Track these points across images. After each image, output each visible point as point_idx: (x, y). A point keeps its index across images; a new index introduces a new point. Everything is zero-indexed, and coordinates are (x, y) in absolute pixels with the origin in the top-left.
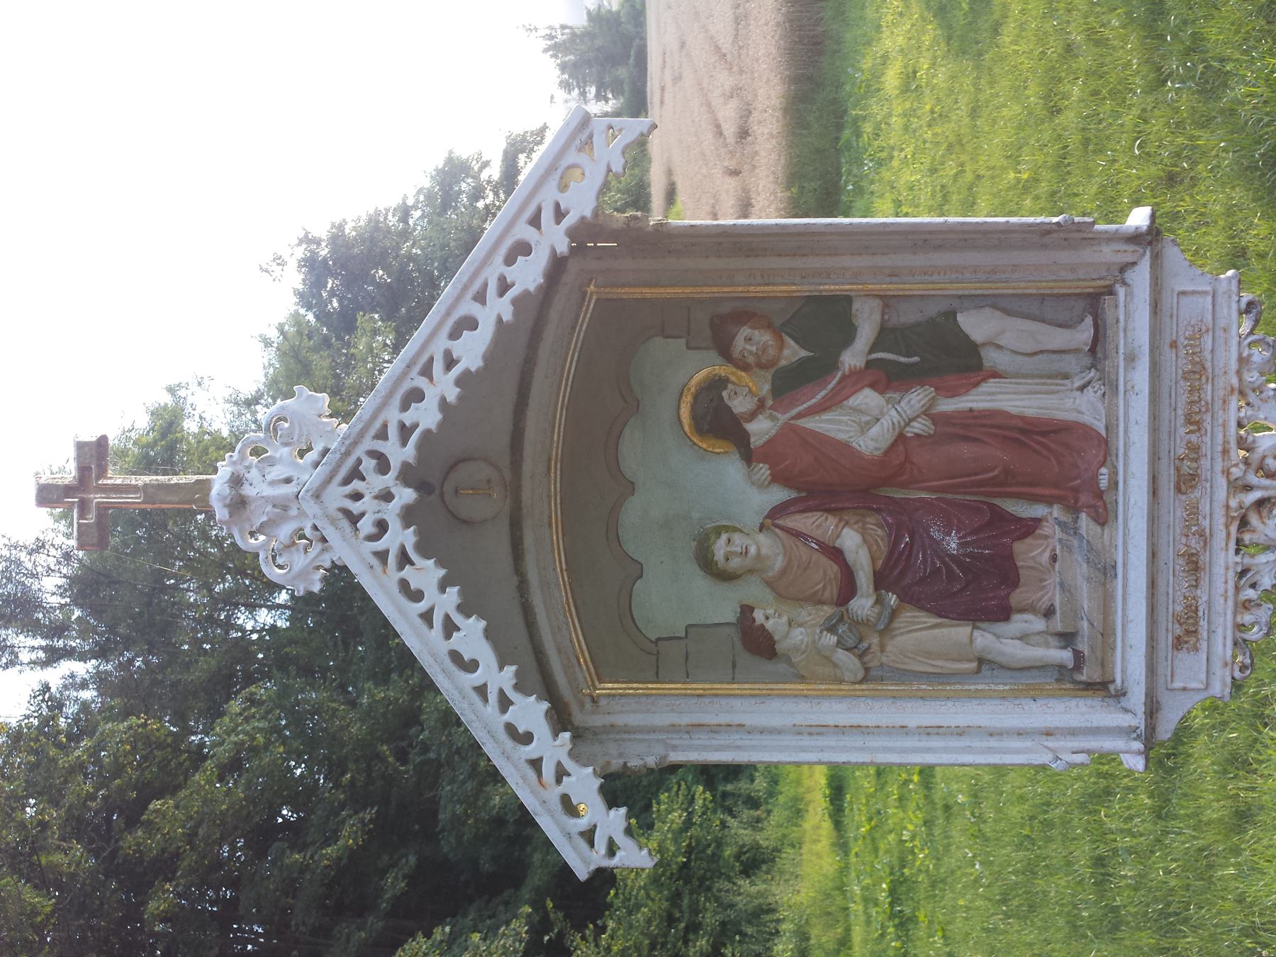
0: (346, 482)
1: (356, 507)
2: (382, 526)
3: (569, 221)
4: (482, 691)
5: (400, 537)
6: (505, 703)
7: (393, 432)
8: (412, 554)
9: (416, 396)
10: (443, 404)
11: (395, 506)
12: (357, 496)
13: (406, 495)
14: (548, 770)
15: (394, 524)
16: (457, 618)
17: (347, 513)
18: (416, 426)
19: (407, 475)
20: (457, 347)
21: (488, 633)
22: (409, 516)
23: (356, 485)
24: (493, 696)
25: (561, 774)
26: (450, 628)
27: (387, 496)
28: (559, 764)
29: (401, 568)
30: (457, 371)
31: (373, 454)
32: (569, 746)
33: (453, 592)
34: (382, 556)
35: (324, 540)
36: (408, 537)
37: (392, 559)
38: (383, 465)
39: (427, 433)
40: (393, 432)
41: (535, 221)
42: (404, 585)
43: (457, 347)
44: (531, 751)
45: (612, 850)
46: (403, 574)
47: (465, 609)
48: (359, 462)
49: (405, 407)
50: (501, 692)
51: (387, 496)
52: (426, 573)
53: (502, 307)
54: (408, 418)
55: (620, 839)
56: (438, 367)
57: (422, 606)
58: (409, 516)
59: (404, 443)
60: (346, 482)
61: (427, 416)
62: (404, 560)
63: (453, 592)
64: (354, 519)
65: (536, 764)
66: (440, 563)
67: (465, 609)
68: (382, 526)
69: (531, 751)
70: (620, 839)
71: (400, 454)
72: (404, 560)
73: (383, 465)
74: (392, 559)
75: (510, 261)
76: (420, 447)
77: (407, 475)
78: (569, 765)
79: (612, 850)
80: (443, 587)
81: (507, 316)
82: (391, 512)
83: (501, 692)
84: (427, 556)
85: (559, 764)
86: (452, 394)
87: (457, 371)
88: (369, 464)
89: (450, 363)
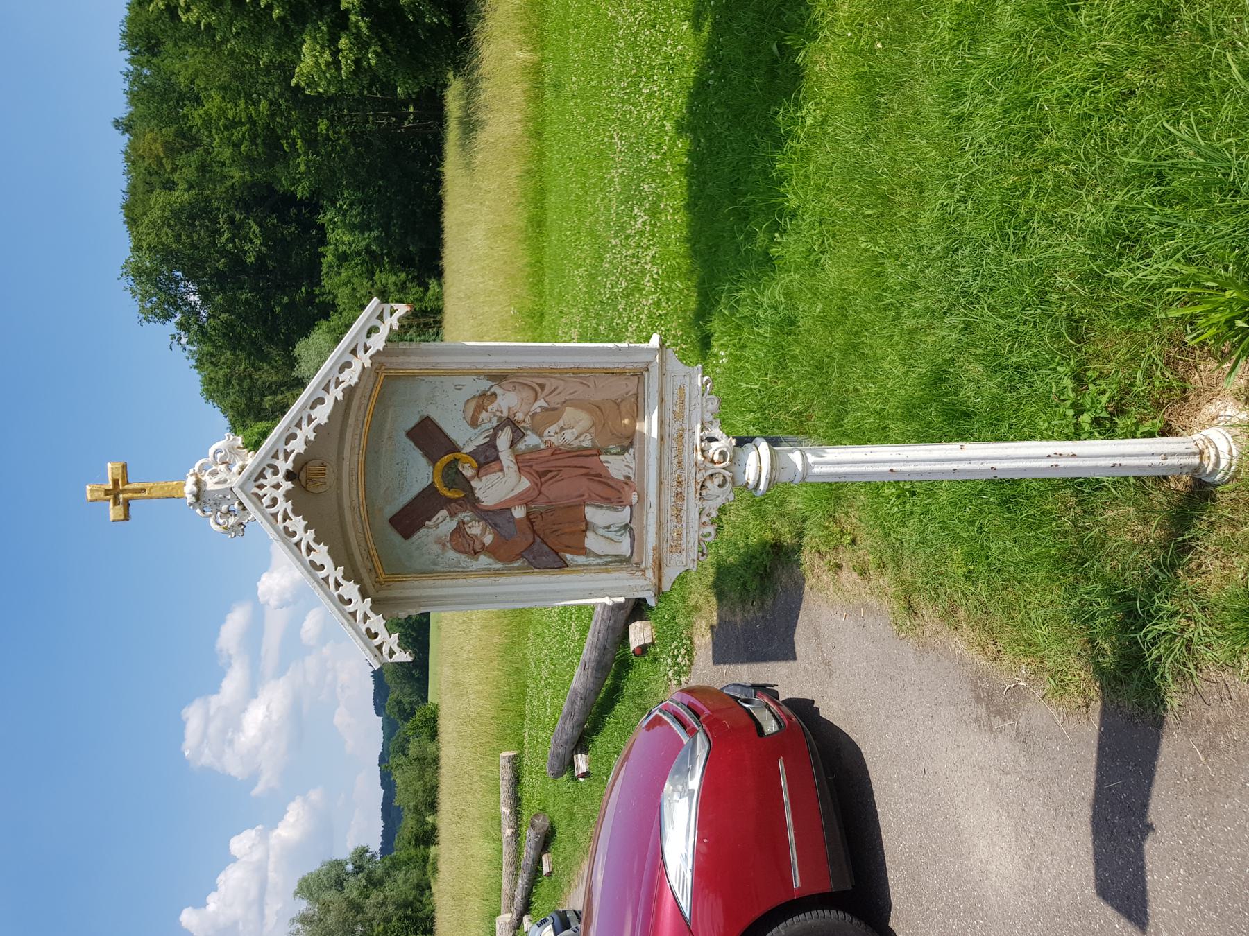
0: (256, 480)
1: (261, 493)
2: (274, 502)
3: (371, 352)
4: (326, 579)
5: (283, 506)
6: (338, 585)
7: (281, 456)
8: (291, 515)
9: (293, 436)
10: (307, 442)
11: (282, 491)
12: (261, 487)
13: (288, 485)
14: (359, 616)
15: (281, 499)
16: (313, 545)
17: (256, 495)
18: (293, 451)
19: (289, 476)
20: (314, 413)
21: (329, 552)
22: (288, 496)
23: (262, 481)
24: (331, 581)
25: (366, 617)
26: (310, 549)
27: (277, 486)
28: (365, 613)
29: (285, 520)
30: (314, 424)
31: (270, 466)
32: (370, 604)
33: (311, 532)
34: (275, 515)
35: (244, 509)
36: (289, 506)
37: (280, 518)
38: (276, 472)
39: (299, 454)
40: (281, 456)
41: (354, 352)
42: (286, 528)
43: (314, 413)
44: (351, 608)
45: (392, 653)
46: (285, 524)
47: (317, 541)
48: (264, 469)
49: (287, 443)
50: (336, 579)
51: (277, 486)
52: (297, 523)
53: (337, 393)
54: (289, 448)
55: (395, 648)
56: (305, 422)
57: (296, 539)
58: (288, 496)
59: (286, 461)
60: (256, 480)
61: (298, 446)
62: (286, 517)
63: (311, 532)
64: (260, 498)
65: (353, 614)
66: (304, 519)
67: (317, 541)
68: (274, 502)
69: (351, 608)
70: (395, 648)
71: (284, 466)
72: (286, 517)
73: (276, 472)
74: (280, 518)
75: (341, 371)
76: (294, 461)
77: (289, 476)
78: (370, 613)
79: (392, 653)
80: (306, 529)
81: (340, 397)
82: (280, 494)
83: (336, 579)
84: (297, 515)
85: (365, 613)
86: (312, 436)
87: (314, 424)
88: (268, 473)
89: (310, 420)
